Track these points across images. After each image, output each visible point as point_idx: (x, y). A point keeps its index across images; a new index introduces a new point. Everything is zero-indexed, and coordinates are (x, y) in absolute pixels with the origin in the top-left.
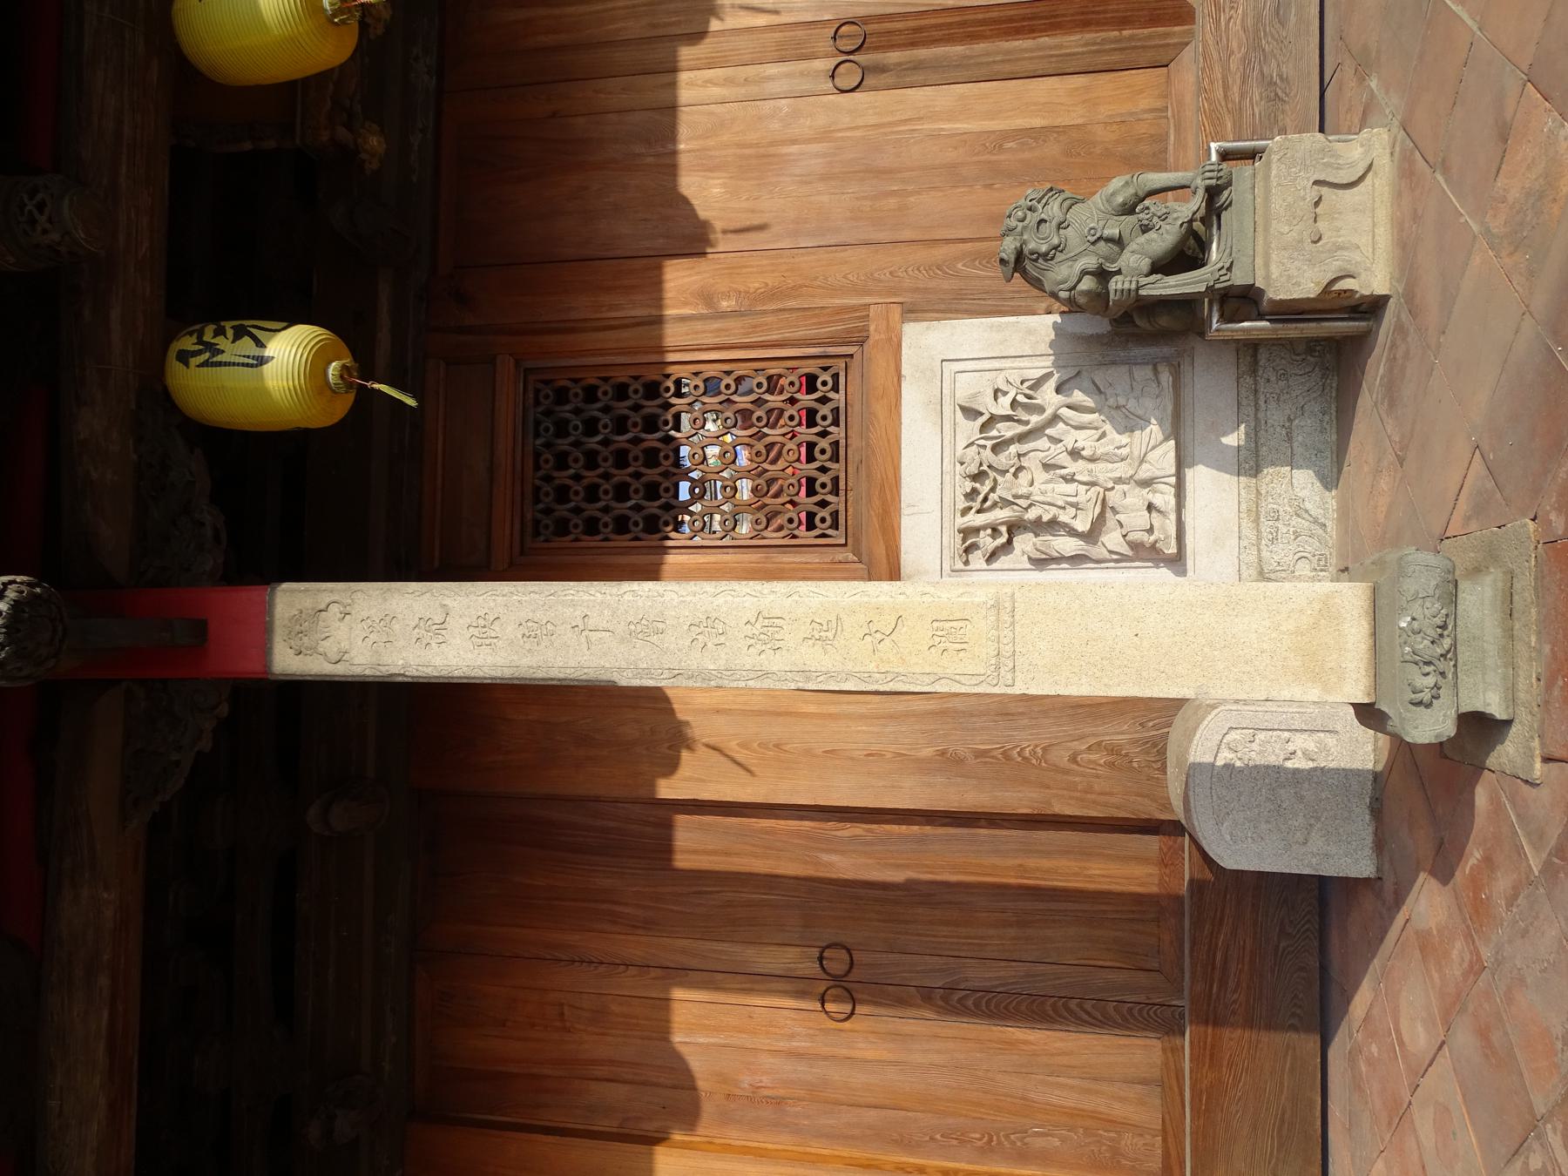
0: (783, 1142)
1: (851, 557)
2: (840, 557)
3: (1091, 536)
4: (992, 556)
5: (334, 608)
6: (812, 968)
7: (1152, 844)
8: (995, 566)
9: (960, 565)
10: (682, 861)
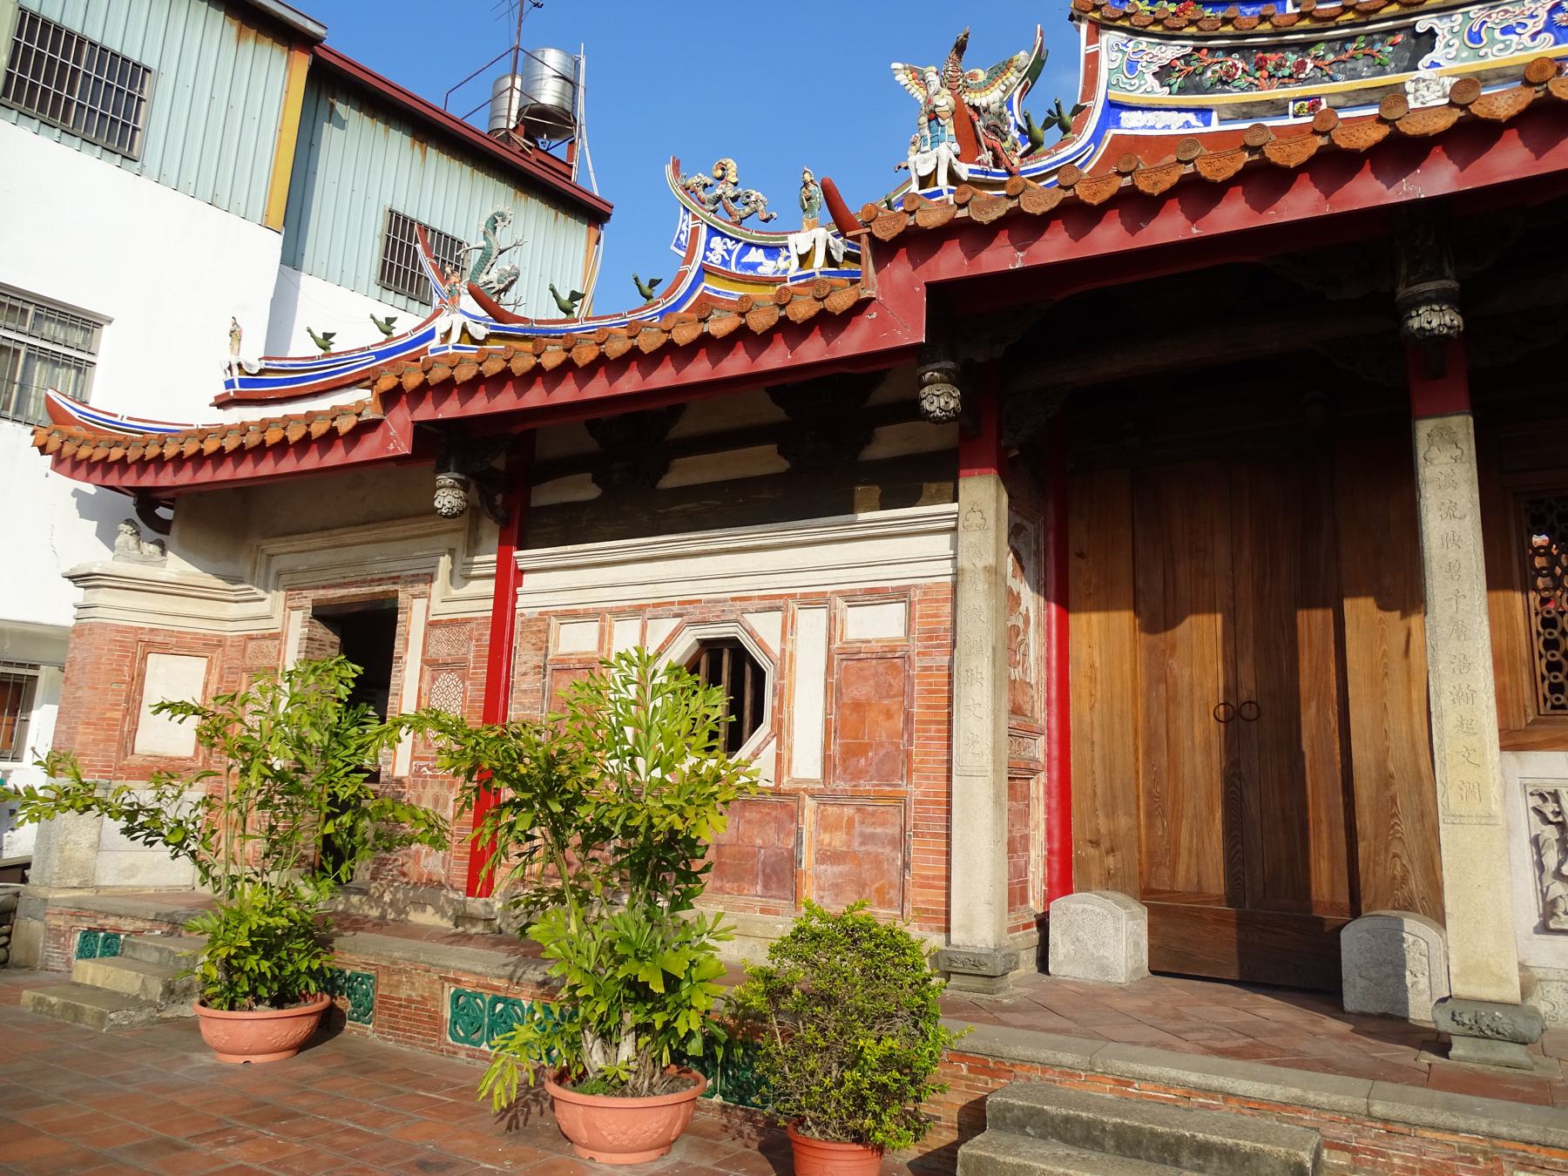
0: (1142, 684)
1: (1530, 719)
2: (1529, 711)
3: (1558, 875)
4: (1537, 811)
5: (1459, 452)
6: (1244, 695)
7: (1344, 899)
8: (1532, 813)
9: (1529, 790)
10: (1302, 616)
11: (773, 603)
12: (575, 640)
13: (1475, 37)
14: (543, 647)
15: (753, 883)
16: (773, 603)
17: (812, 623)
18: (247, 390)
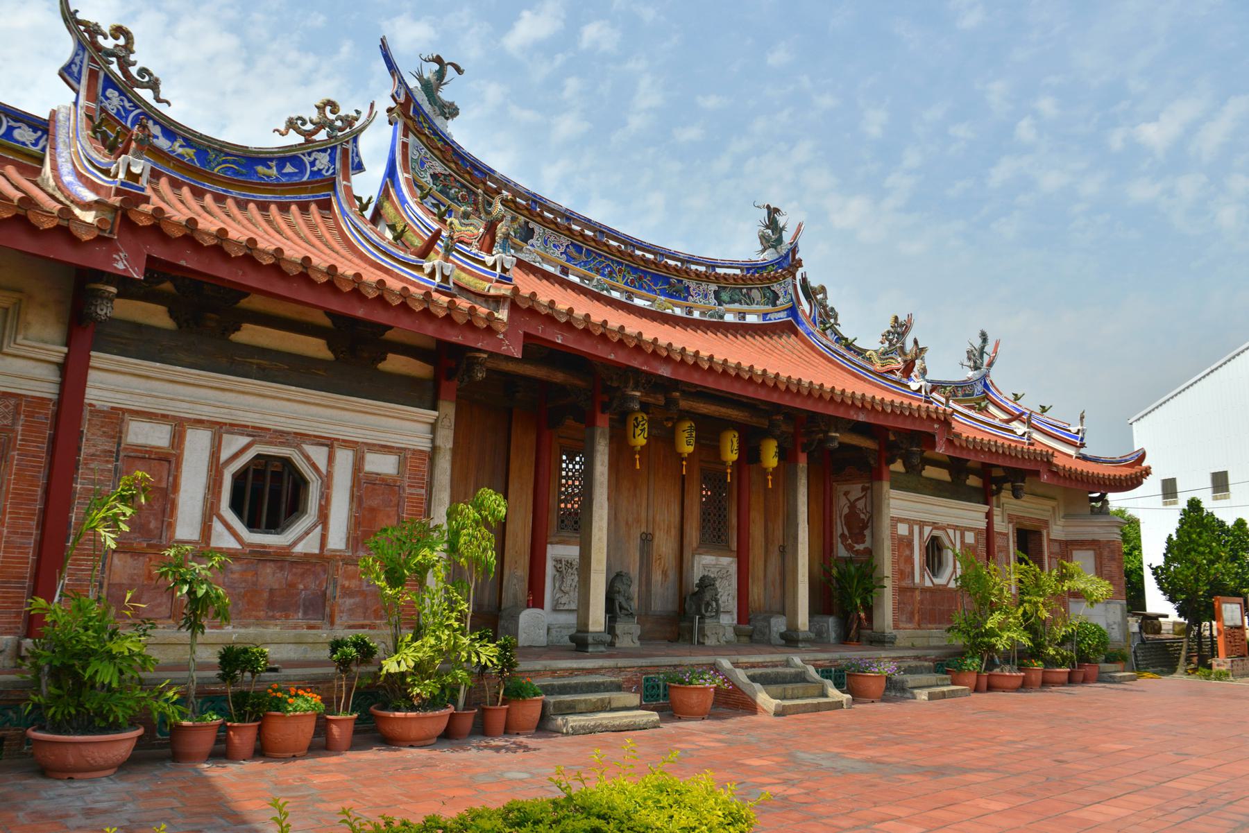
11: (330, 444)
13: (546, 242)
14: (118, 436)
15: (297, 611)
16: (320, 441)
17: (344, 459)
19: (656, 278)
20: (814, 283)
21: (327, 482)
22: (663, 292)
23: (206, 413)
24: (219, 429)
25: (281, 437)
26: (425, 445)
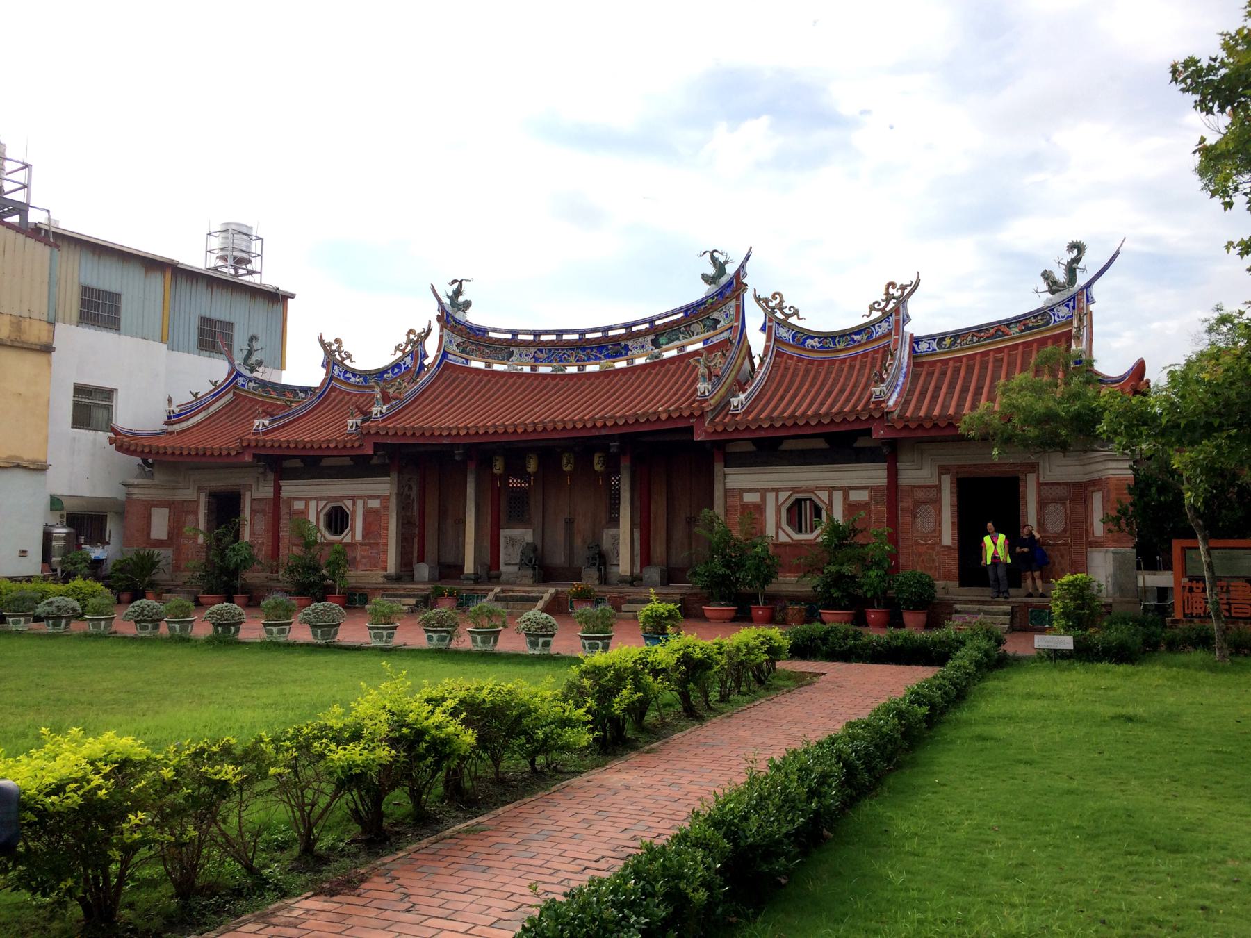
12: (299, 505)
16: (349, 498)
17: (360, 503)
18: (172, 418)
19: (600, 349)
20: (766, 293)
21: (354, 512)
22: (607, 356)
23: (313, 494)
24: (318, 499)
25: (336, 499)
26: (387, 493)
